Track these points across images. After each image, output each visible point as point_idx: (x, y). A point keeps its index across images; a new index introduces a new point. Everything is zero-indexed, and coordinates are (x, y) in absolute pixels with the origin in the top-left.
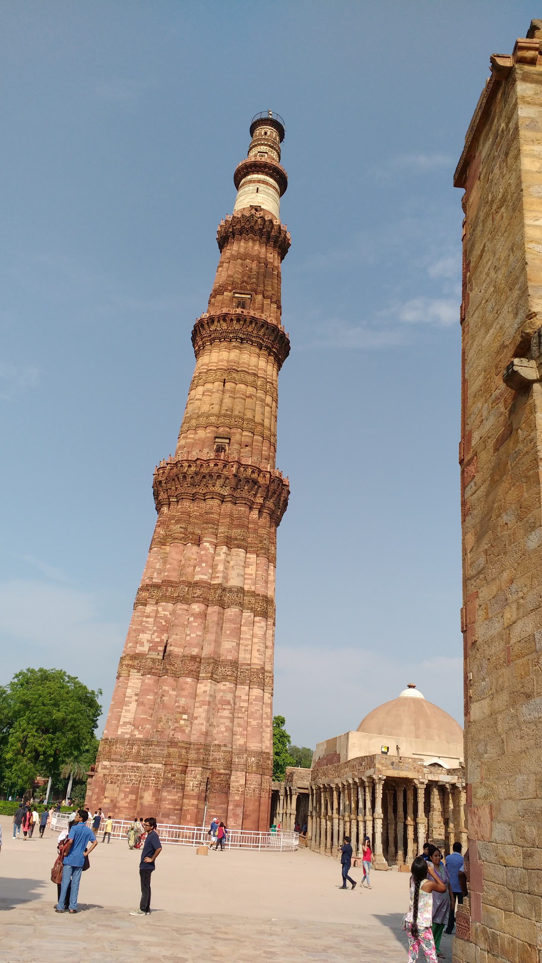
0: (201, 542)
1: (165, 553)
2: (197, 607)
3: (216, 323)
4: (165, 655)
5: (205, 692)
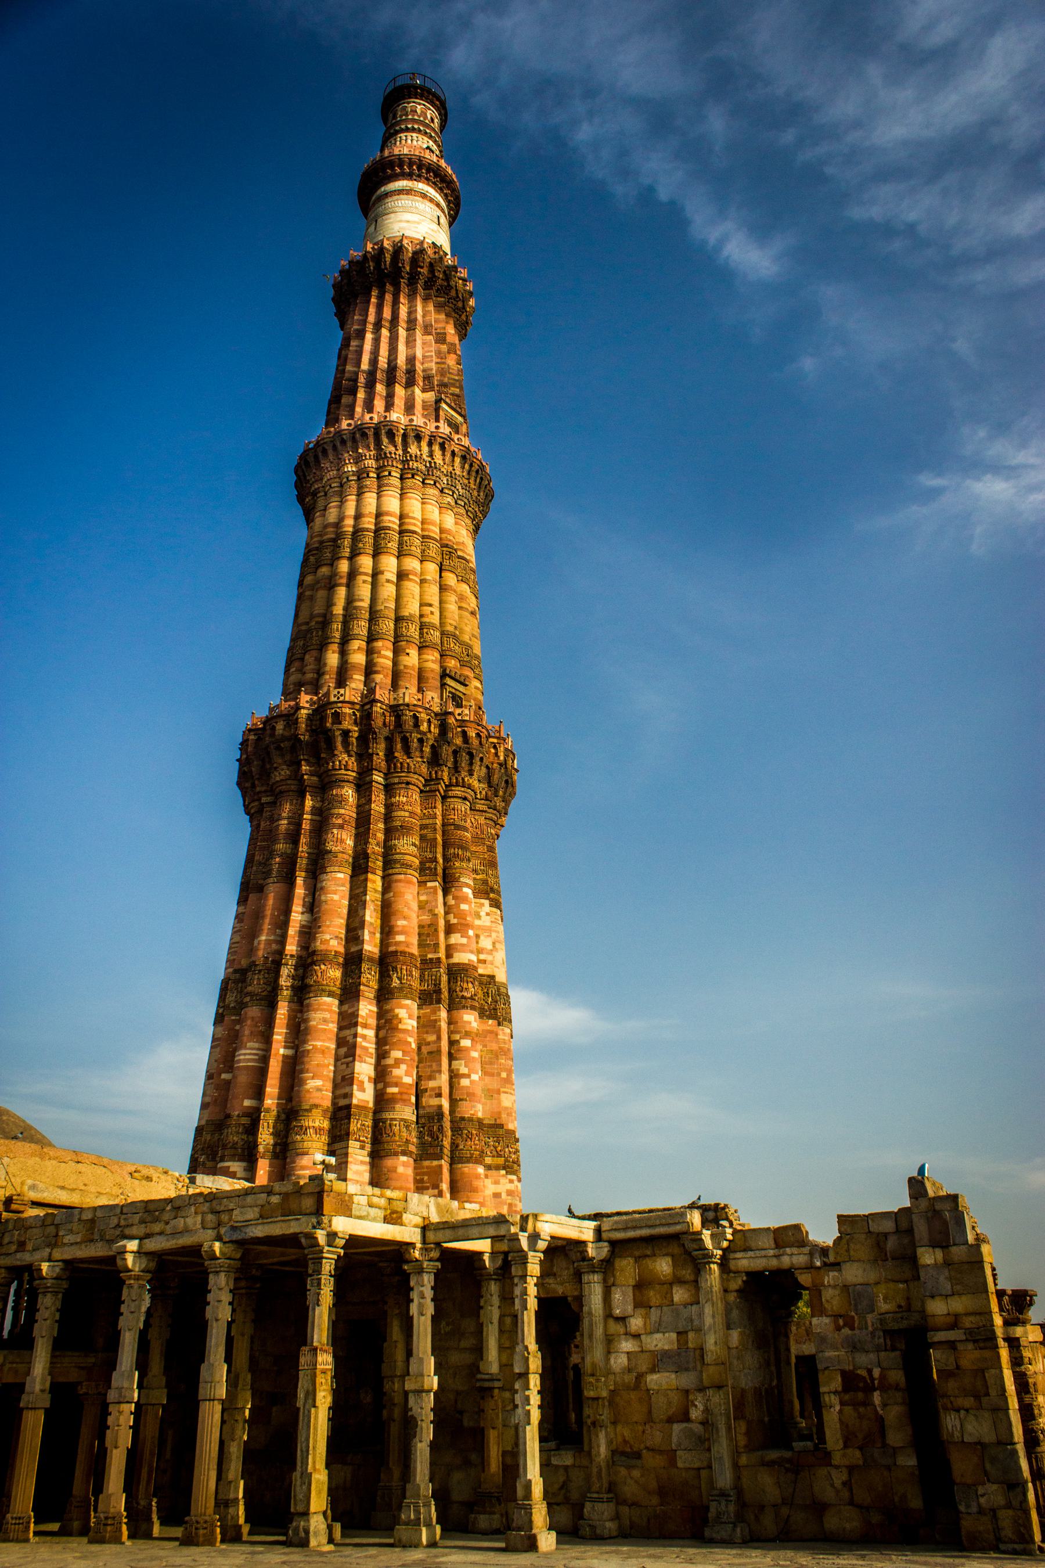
0: (456, 884)
1: (376, 891)
2: (470, 1018)
3: (424, 444)
4: (421, 1112)
5: (497, 1195)
